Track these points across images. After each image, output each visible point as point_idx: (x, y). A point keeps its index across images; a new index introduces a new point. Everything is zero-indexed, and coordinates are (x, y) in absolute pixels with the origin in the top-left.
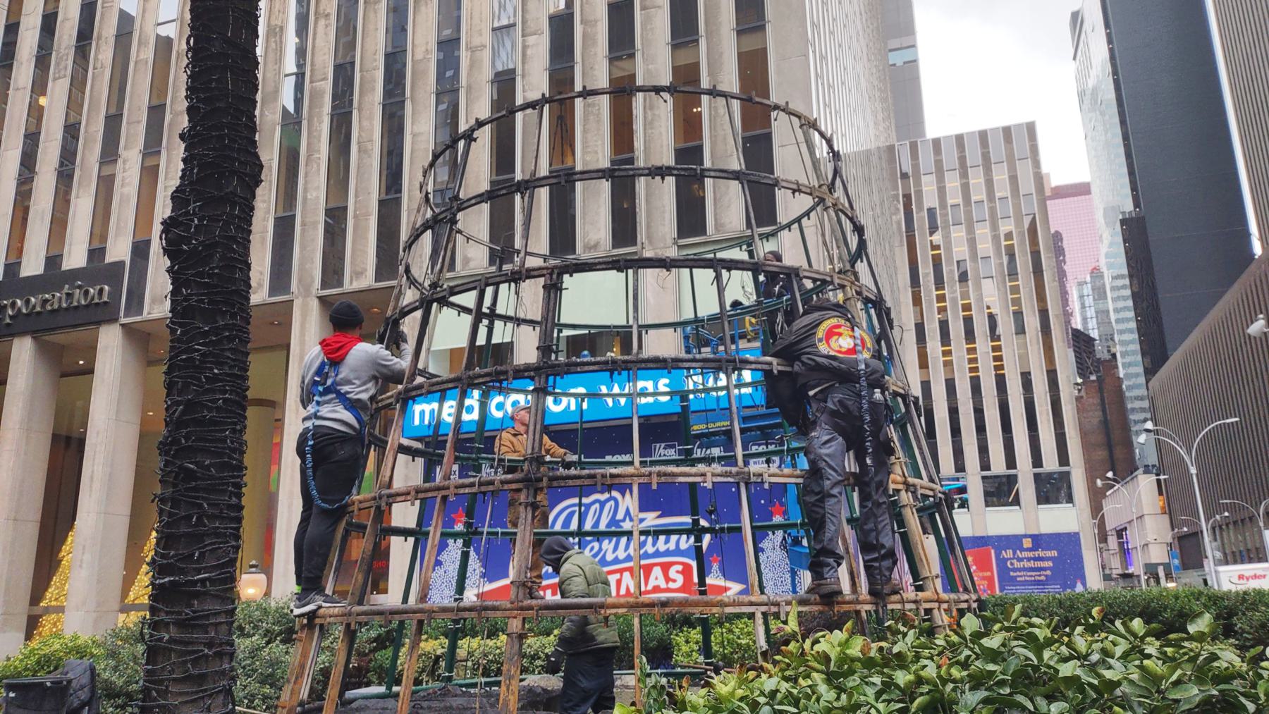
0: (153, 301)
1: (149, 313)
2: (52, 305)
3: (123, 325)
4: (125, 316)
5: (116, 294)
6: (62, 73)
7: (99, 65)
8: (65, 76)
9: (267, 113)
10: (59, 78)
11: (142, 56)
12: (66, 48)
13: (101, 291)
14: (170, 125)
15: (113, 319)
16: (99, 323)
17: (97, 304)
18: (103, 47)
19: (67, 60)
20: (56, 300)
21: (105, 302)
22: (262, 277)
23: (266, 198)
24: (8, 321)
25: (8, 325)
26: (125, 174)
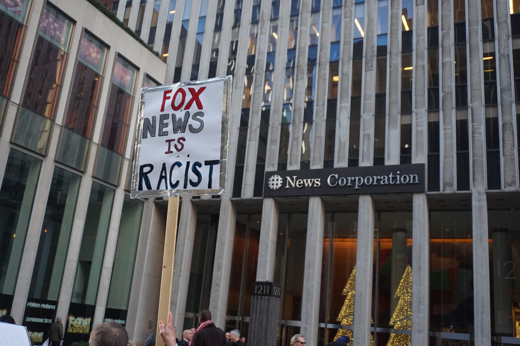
0: (445, 185)
1: (444, 191)
2: (384, 182)
3: (428, 196)
4: (428, 191)
5: (422, 179)
6: (370, 68)
7: (393, 66)
8: (372, 70)
9: (505, 96)
10: (369, 70)
11: (420, 63)
12: (371, 56)
13: (414, 177)
14: (443, 98)
15: (422, 191)
16: (413, 193)
17: (412, 184)
18: (394, 57)
19: (372, 62)
20: (386, 179)
21: (417, 184)
22: (514, 178)
23: (511, 139)
24: (357, 187)
25: (357, 189)
26: (418, 120)
